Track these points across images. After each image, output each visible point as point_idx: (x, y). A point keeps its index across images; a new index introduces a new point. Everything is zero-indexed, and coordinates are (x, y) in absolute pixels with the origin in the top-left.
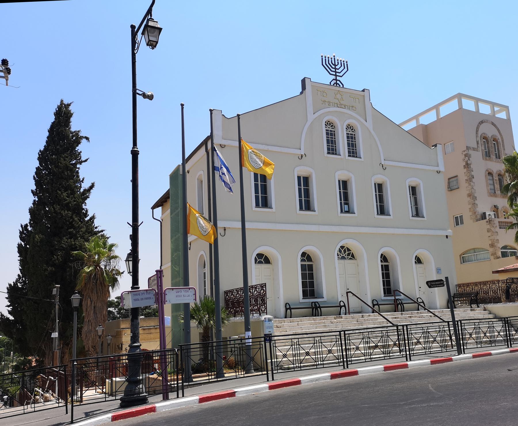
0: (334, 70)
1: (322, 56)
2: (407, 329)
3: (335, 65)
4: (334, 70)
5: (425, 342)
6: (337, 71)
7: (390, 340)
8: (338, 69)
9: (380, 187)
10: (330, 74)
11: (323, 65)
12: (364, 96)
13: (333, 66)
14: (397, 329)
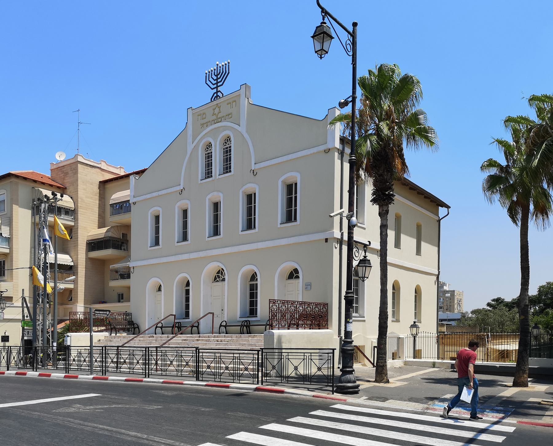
1: (206, 74)
2: (149, 350)
3: (217, 76)
4: (216, 82)
5: (178, 366)
7: (134, 359)
9: (250, 198)
10: (212, 89)
13: (219, 77)
14: (157, 350)
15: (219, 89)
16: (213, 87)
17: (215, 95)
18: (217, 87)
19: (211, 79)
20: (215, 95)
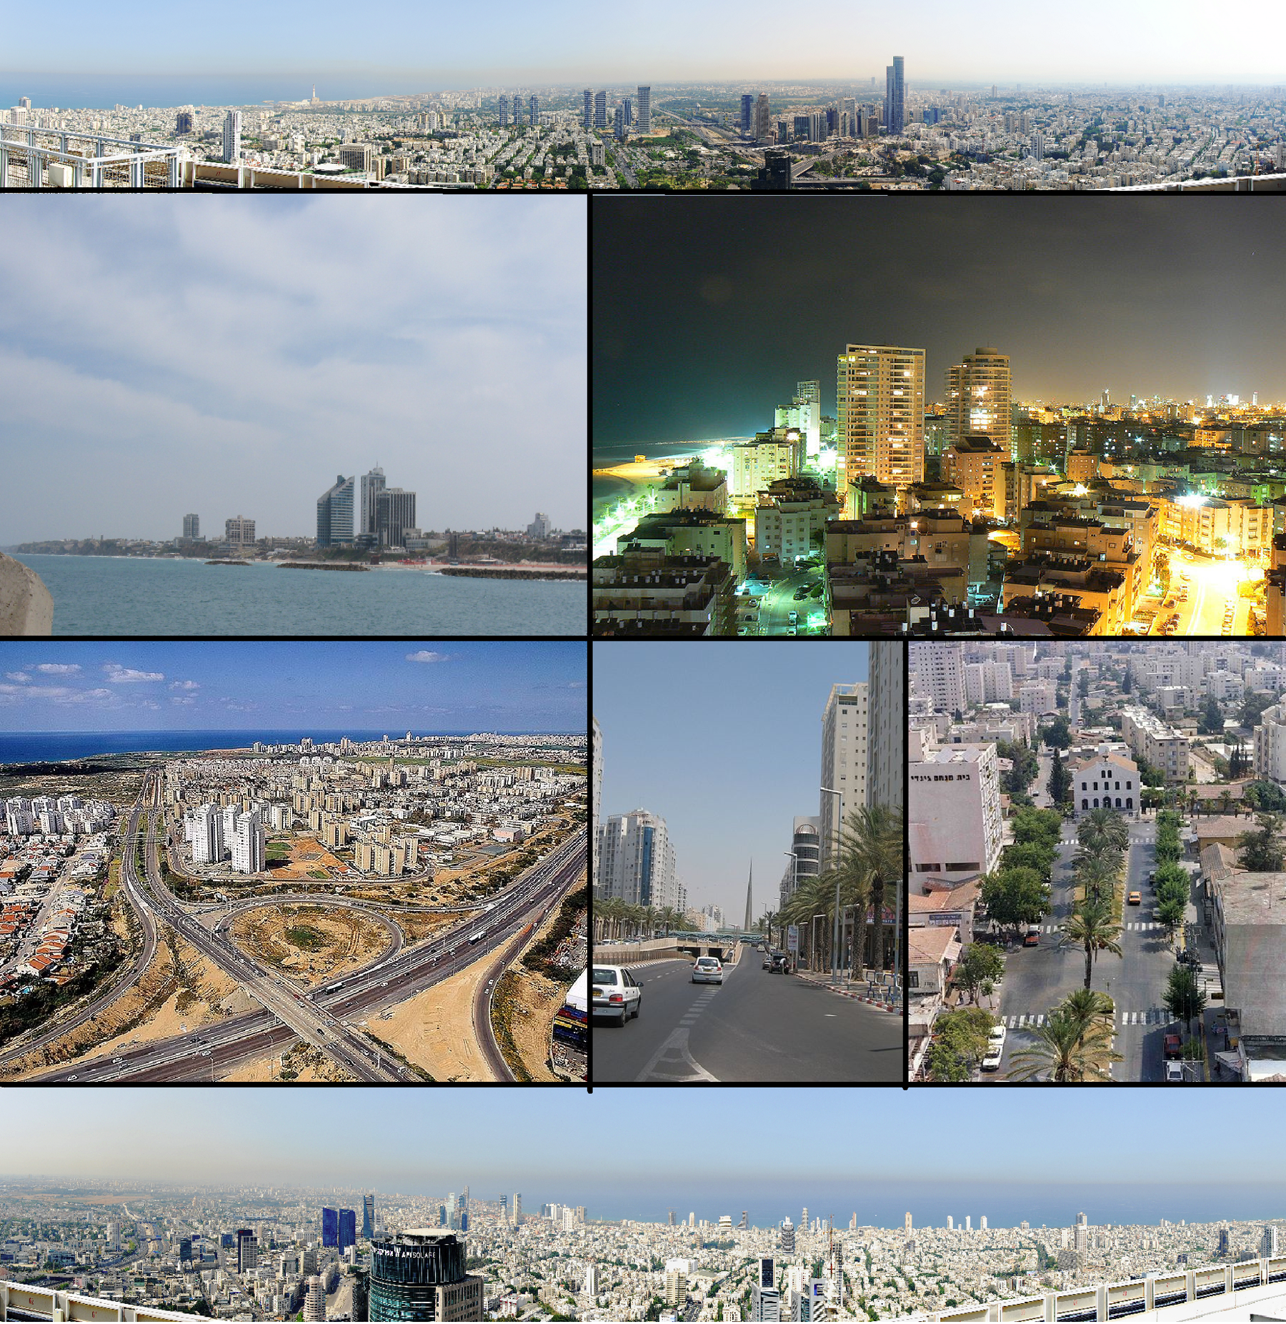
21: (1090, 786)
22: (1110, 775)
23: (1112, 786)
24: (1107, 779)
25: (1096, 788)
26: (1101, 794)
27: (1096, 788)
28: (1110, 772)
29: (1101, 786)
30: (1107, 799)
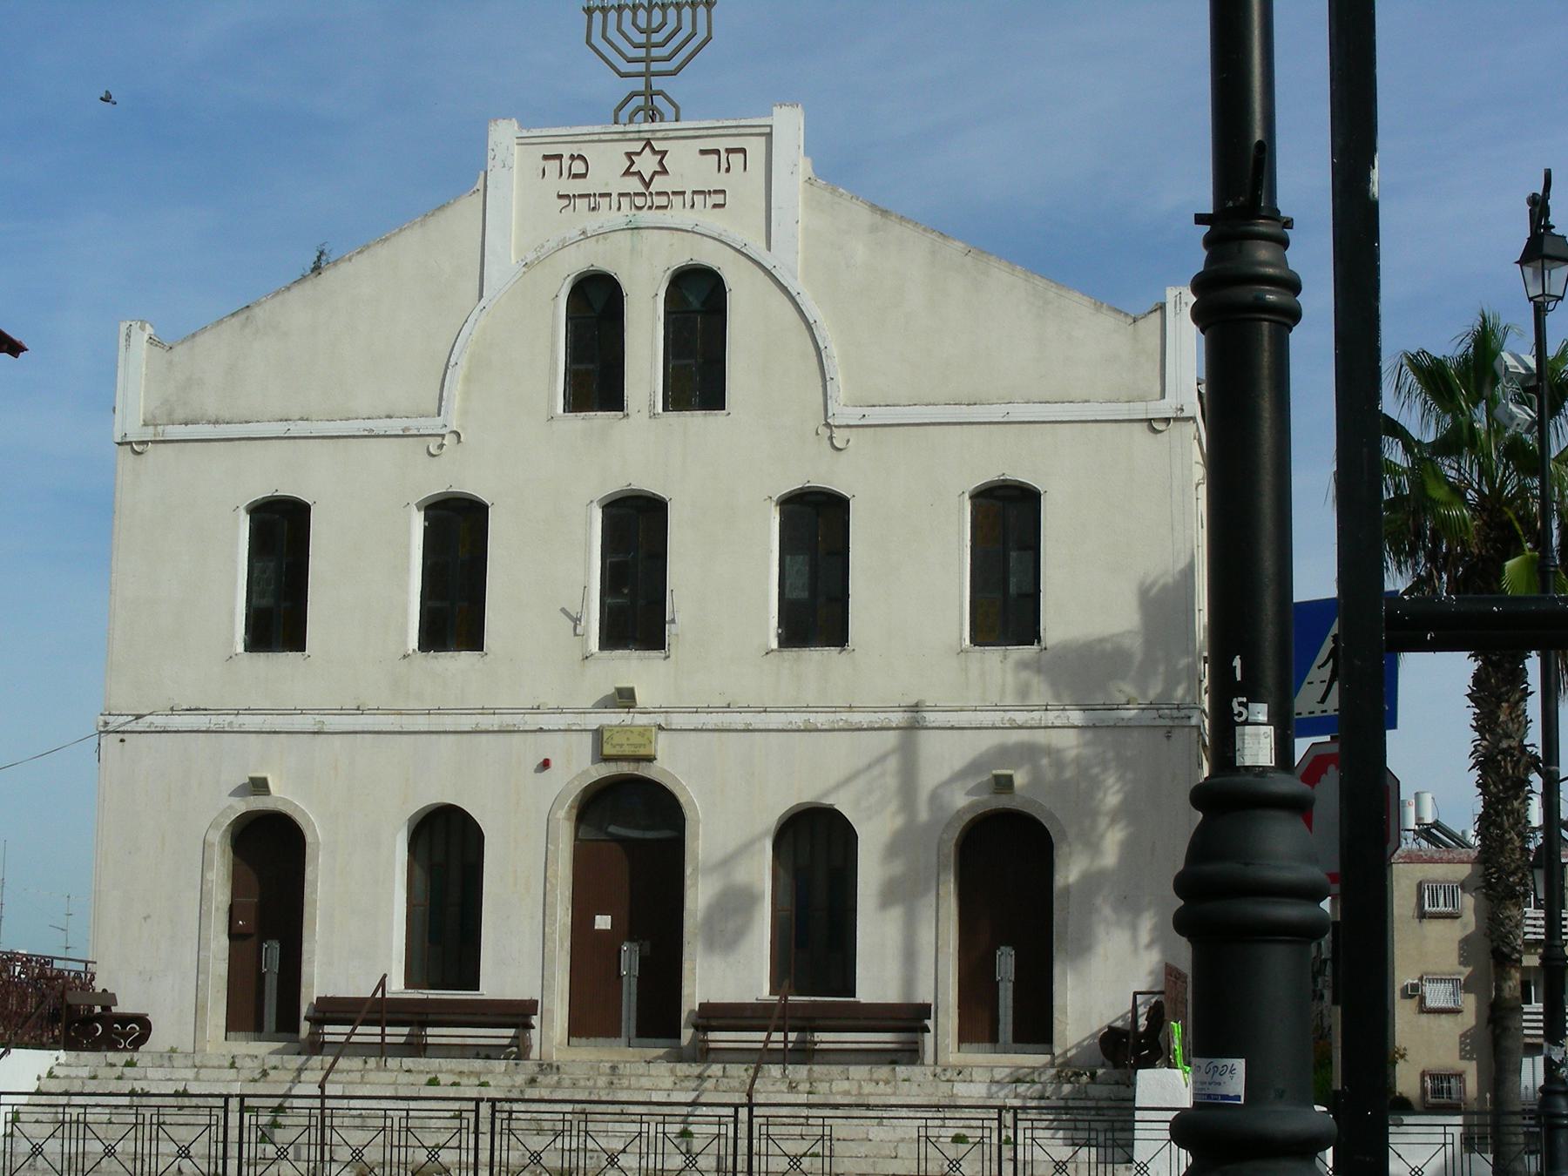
0: (642, 53)
3: (648, 31)
4: (642, 53)
6: (655, 52)
8: (662, 45)
10: (623, 75)
11: (588, 42)
12: (770, 134)
15: (657, 84)
16: (625, 67)
17: (639, 101)
18: (648, 74)
19: (612, 33)
20: (639, 101)
21: (368, 576)
22: (698, 378)
23: (726, 573)
24: (644, 443)
25: (453, 609)
26: (515, 736)
27: (453, 609)
28: (698, 301)
29: (545, 572)
30: (630, 834)
